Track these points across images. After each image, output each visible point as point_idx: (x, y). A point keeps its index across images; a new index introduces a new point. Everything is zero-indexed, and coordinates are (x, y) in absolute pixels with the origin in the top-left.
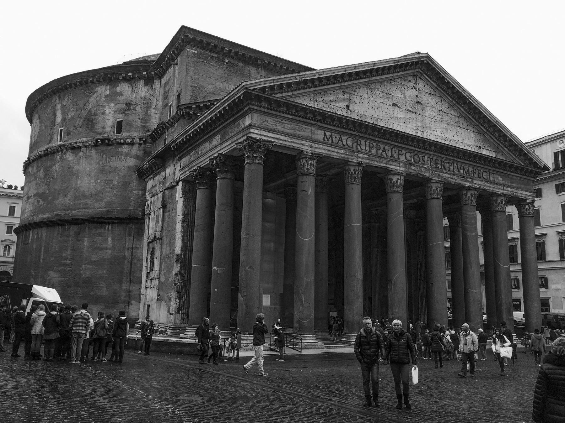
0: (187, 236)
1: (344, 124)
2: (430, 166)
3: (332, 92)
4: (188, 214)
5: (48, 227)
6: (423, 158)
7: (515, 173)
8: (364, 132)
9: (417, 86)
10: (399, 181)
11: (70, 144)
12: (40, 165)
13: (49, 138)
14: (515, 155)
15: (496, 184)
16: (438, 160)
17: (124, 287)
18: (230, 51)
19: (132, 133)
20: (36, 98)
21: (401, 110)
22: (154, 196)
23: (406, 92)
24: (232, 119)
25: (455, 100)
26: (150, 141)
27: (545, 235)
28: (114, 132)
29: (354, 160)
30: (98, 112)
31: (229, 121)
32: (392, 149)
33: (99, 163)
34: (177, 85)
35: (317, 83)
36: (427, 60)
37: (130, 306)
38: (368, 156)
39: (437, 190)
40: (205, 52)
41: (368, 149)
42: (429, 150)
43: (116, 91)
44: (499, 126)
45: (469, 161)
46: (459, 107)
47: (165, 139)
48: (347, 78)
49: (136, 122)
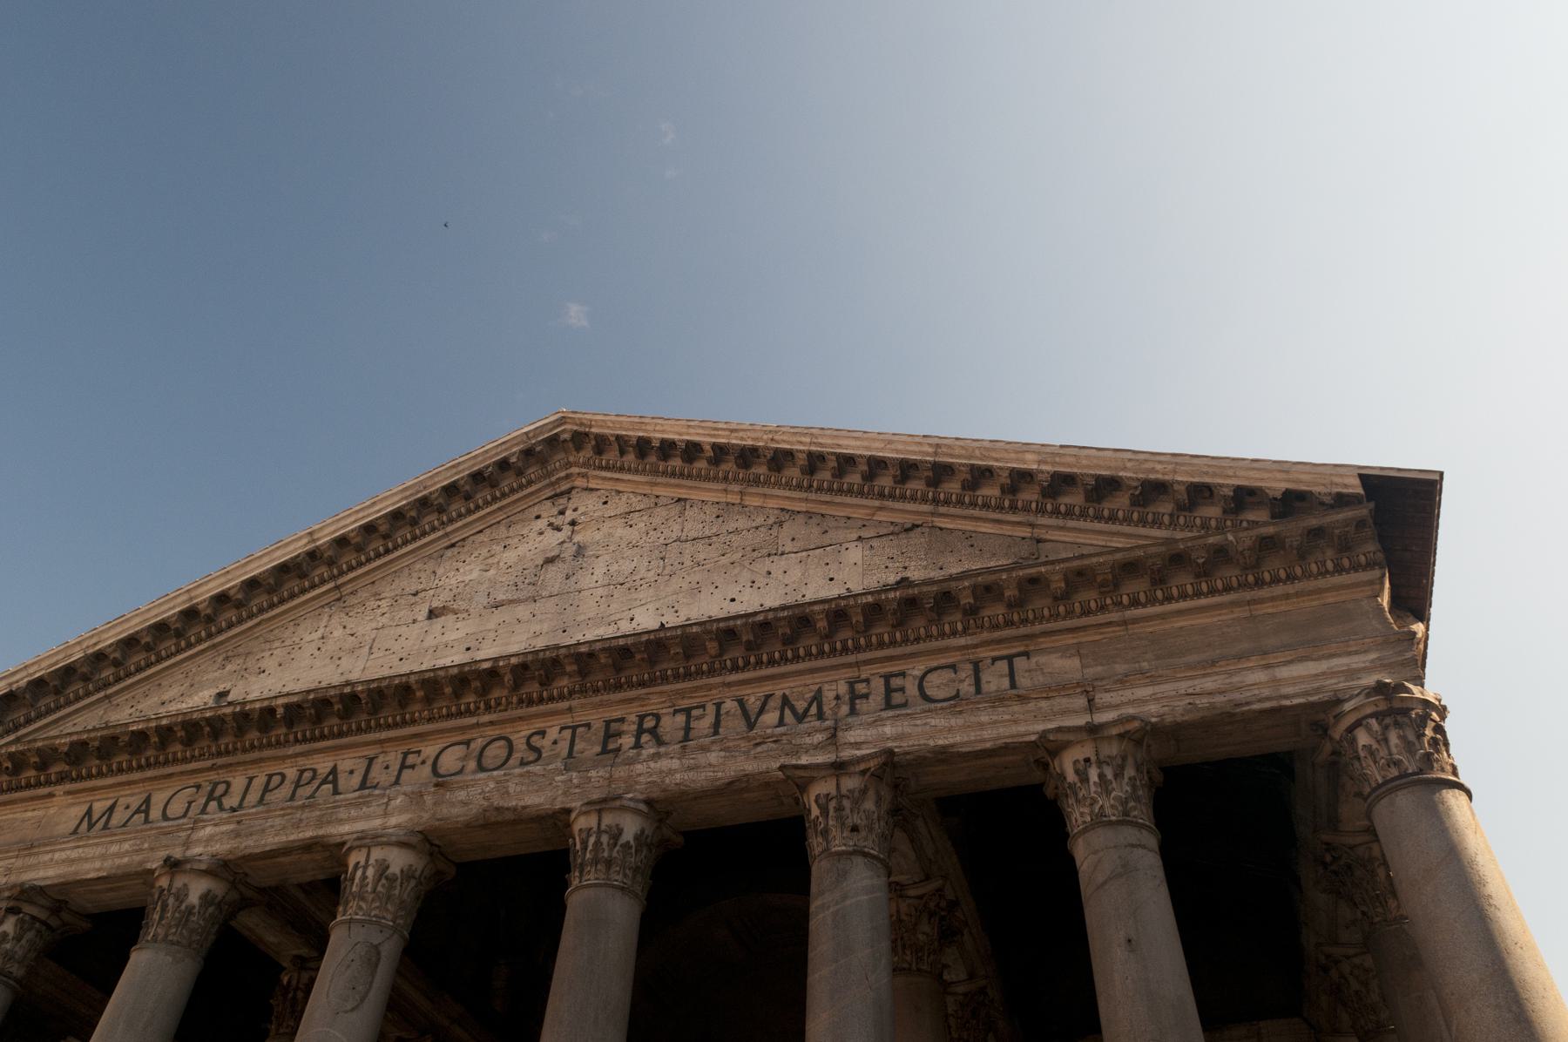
1: (150, 753)
2: (570, 755)
3: (181, 676)
7: (1169, 599)
10: (359, 873)
14: (1156, 523)
15: (1022, 699)
16: (622, 720)
21: (465, 615)
23: (505, 555)
38: (231, 827)
39: (585, 848)
41: (253, 797)
42: (551, 699)
44: (959, 457)
46: (766, 490)
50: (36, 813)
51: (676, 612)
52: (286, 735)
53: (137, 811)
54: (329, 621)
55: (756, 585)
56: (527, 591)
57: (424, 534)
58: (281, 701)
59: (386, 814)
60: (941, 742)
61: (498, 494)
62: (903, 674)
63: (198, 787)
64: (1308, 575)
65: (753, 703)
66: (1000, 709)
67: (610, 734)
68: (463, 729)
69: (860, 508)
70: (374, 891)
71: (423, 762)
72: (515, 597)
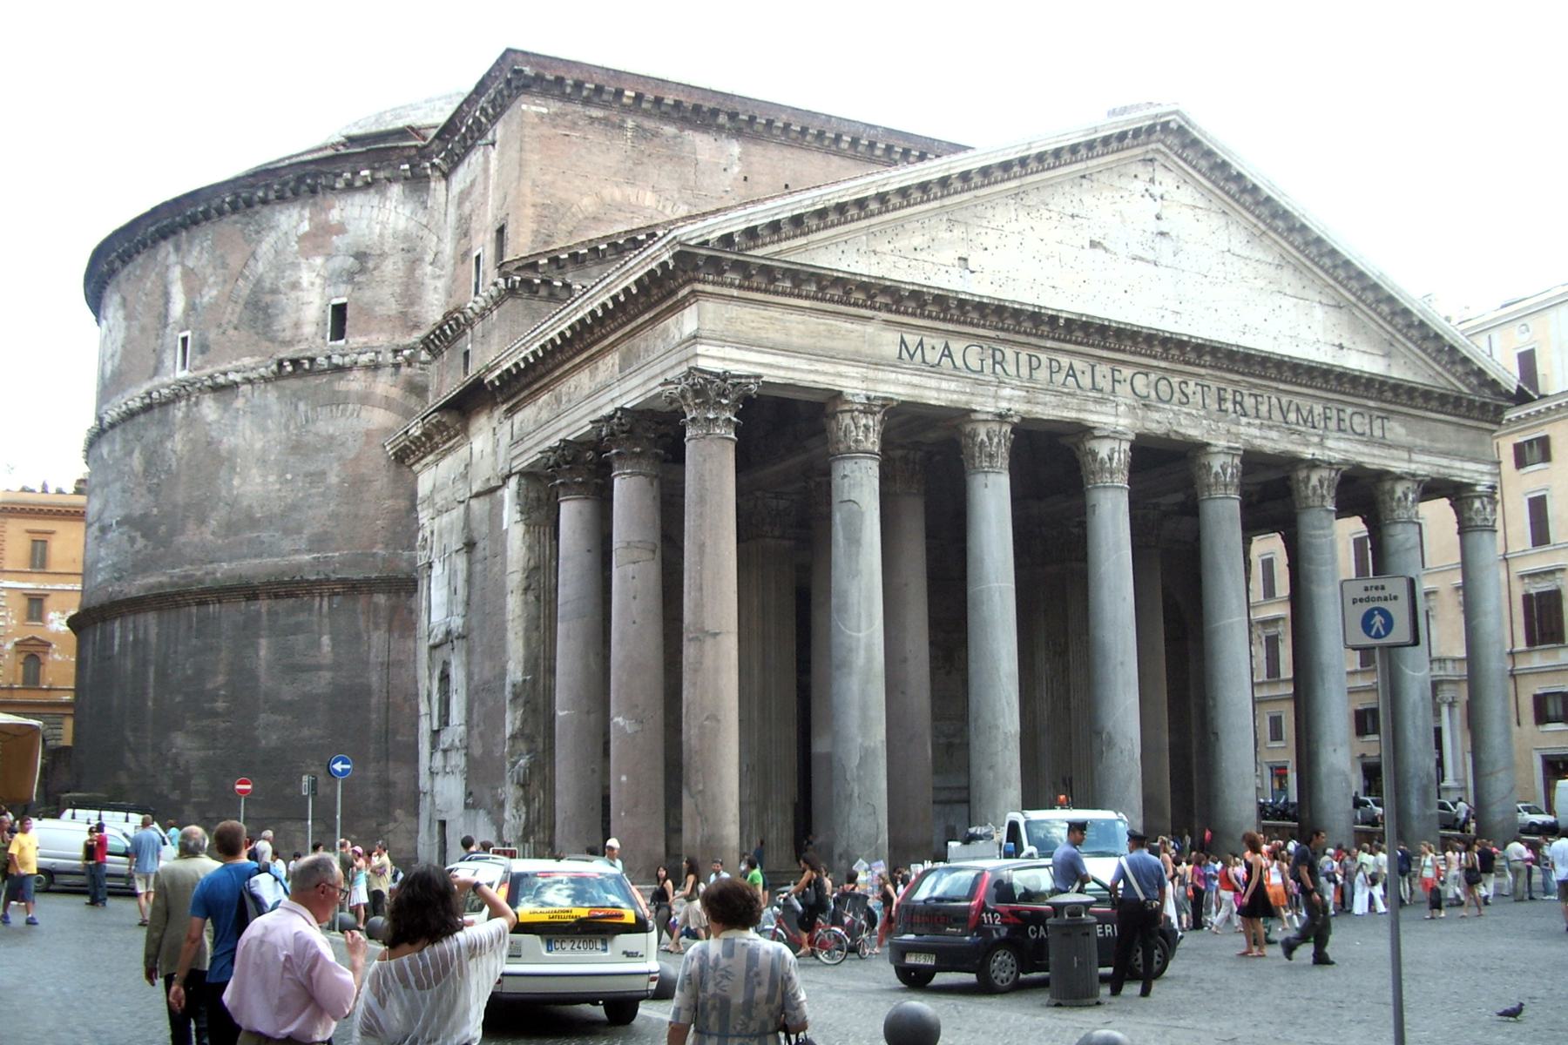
0: (538, 627)
1: (953, 311)
2: (1204, 406)
3: (919, 225)
4: (537, 568)
5: (160, 609)
6: (1183, 386)
7: (1441, 412)
10: (1116, 455)
11: (211, 377)
12: (130, 436)
13: (152, 362)
15: (1390, 446)
17: (374, 774)
18: (639, 97)
19: (374, 337)
20: (115, 251)
22: (440, 513)
24: (647, 316)
25: (1264, 222)
26: (424, 356)
27: (1562, 570)
28: (324, 338)
29: (985, 404)
30: (282, 284)
31: (640, 320)
32: (1093, 367)
33: (287, 427)
34: (494, 200)
35: (874, 206)
36: (1178, 119)
37: (391, 826)
38: (1024, 394)
39: (1225, 474)
40: (570, 108)
41: (1024, 371)
42: (1198, 365)
43: (327, 222)
45: (1310, 387)
47: (467, 353)
48: (958, 185)
49: (382, 304)
50: (854, 326)
53: (943, 355)
56: (1150, 256)
57: (1076, 162)
58: (1065, 315)
60: (1359, 459)
64: (1482, 420)
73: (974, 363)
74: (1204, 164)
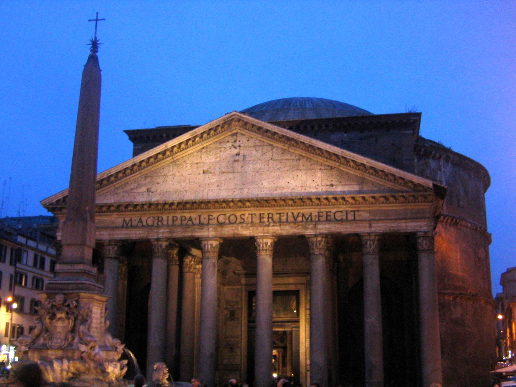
2: (252, 222)
3: (134, 181)
6: (242, 216)
7: (390, 203)
8: (162, 209)
9: (238, 143)
10: (206, 246)
14: (391, 181)
15: (356, 223)
16: (263, 214)
21: (214, 174)
23: (222, 154)
25: (287, 143)
29: (153, 236)
38: (168, 230)
41: (170, 222)
42: (246, 207)
46: (295, 148)
51: (274, 184)
52: (177, 208)
53: (139, 222)
54: (173, 168)
55: (294, 179)
56: (231, 170)
57: (196, 144)
58: (176, 202)
59: (209, 232)
60: (339, 231)
61: (216, 134)
62: (330, 212)
63: (154, 217)
64: (418, 202)
65: (296, 214)
66: (352, 225)
67: (261, 217)
68: (223, 211)
69: (321, 160)
70: (211, 250)
71: (214, 218)
72: (228, 171)
73: (150, 223)
74: (255, 129)
